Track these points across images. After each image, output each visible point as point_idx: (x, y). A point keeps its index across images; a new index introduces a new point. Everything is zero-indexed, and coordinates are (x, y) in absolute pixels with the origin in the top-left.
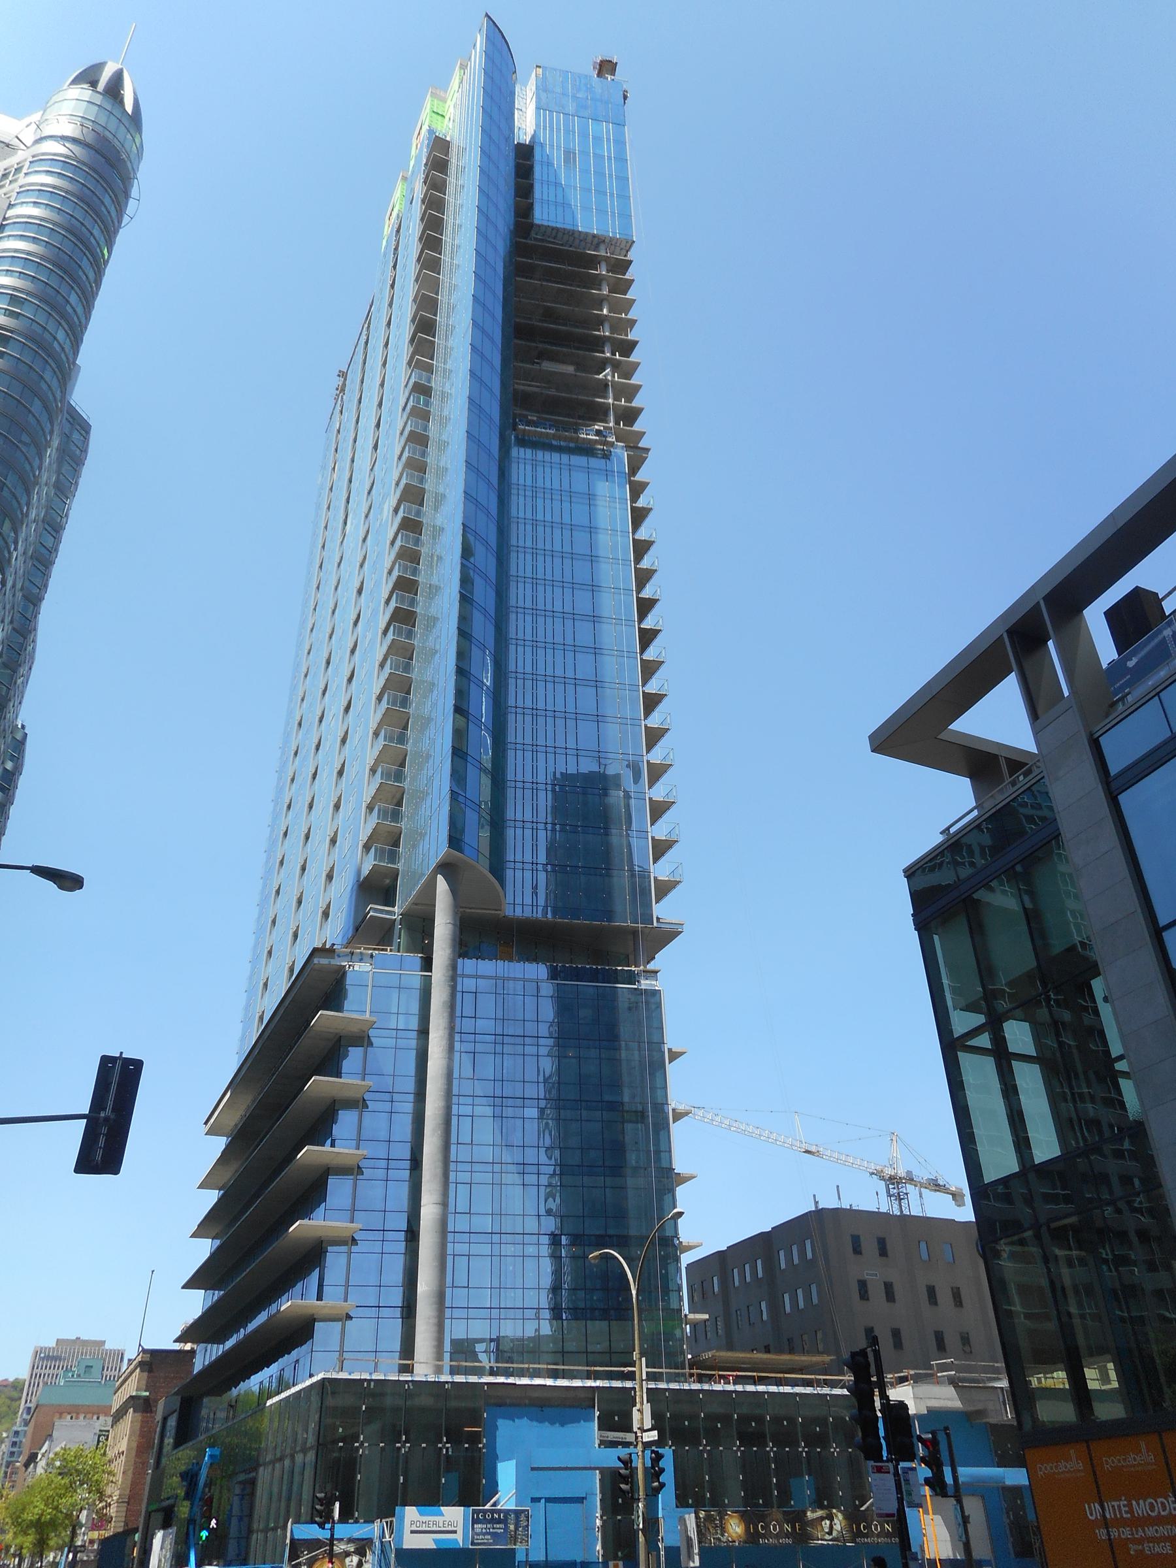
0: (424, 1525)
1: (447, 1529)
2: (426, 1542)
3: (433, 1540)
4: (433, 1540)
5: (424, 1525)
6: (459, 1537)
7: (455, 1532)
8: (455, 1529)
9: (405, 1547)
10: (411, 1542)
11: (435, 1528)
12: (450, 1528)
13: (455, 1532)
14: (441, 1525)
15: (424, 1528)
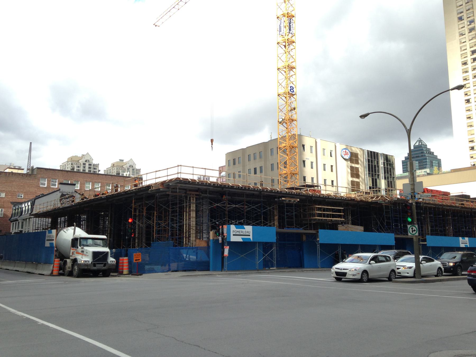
0: (238, 232)
1: (246, 234)
2: (239, 239)
3: (242, 238)
4: (242, 238)
5: (238, 232)
6: (251, 237)
7: (249, 235)
8: (249, 234)
9: (231, 241)
10: (234, 239)
11: (242, 234)
12: (247, 234)
13: (249, 235)
14: (244, 232)
15: (238, 234)
